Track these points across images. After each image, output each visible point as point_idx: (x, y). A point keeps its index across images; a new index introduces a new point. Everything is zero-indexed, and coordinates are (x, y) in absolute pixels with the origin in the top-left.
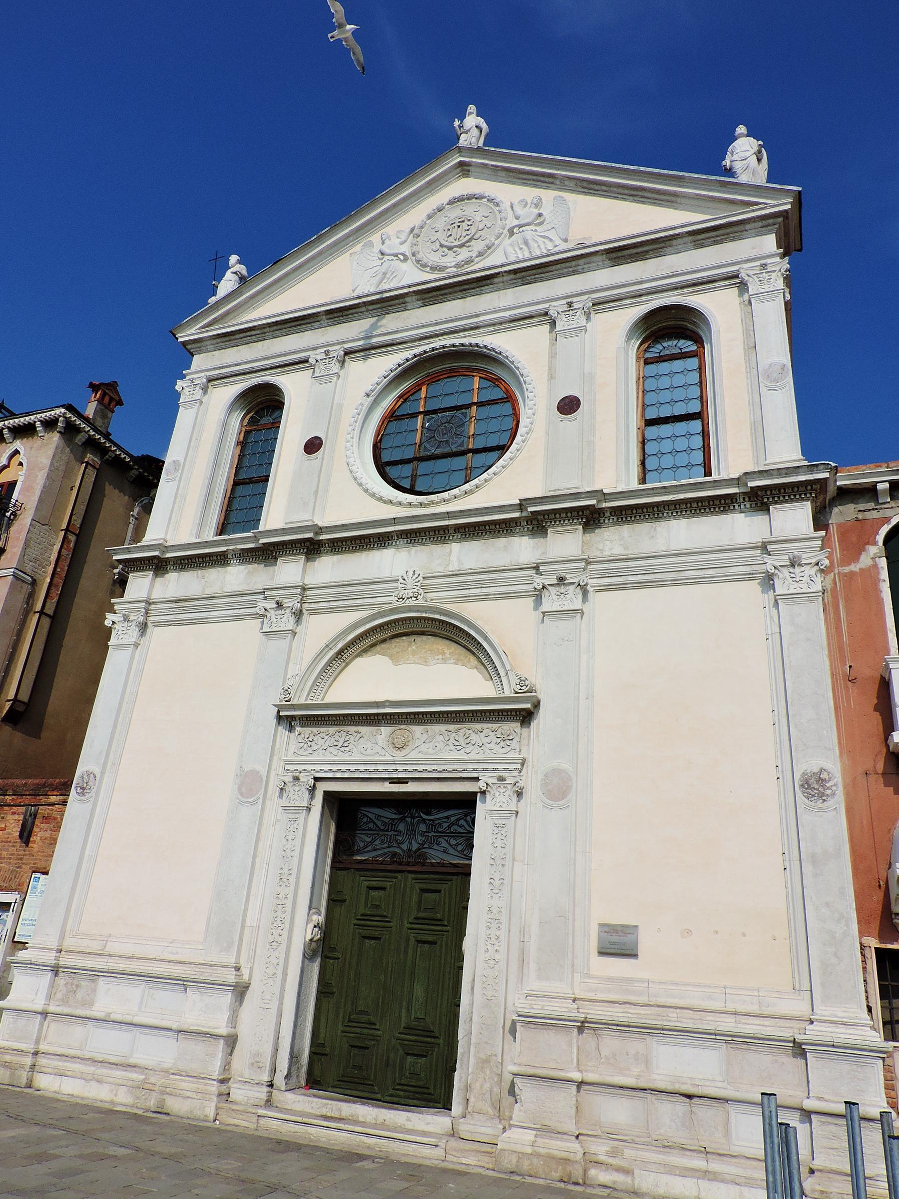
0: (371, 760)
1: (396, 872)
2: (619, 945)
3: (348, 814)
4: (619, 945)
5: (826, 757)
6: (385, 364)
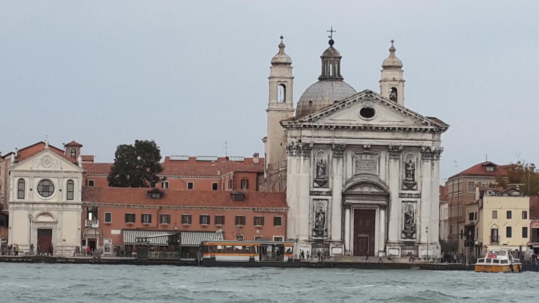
0: (42, 226)
1: (45, 235)
2: (64, 240)
3: (39, 231)
4: (64, 240)
5: (80, 227)
6: (40, 179)
